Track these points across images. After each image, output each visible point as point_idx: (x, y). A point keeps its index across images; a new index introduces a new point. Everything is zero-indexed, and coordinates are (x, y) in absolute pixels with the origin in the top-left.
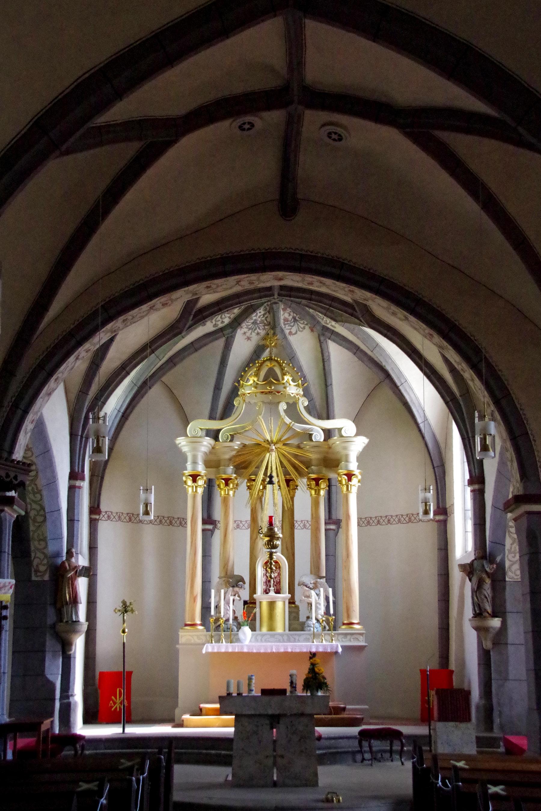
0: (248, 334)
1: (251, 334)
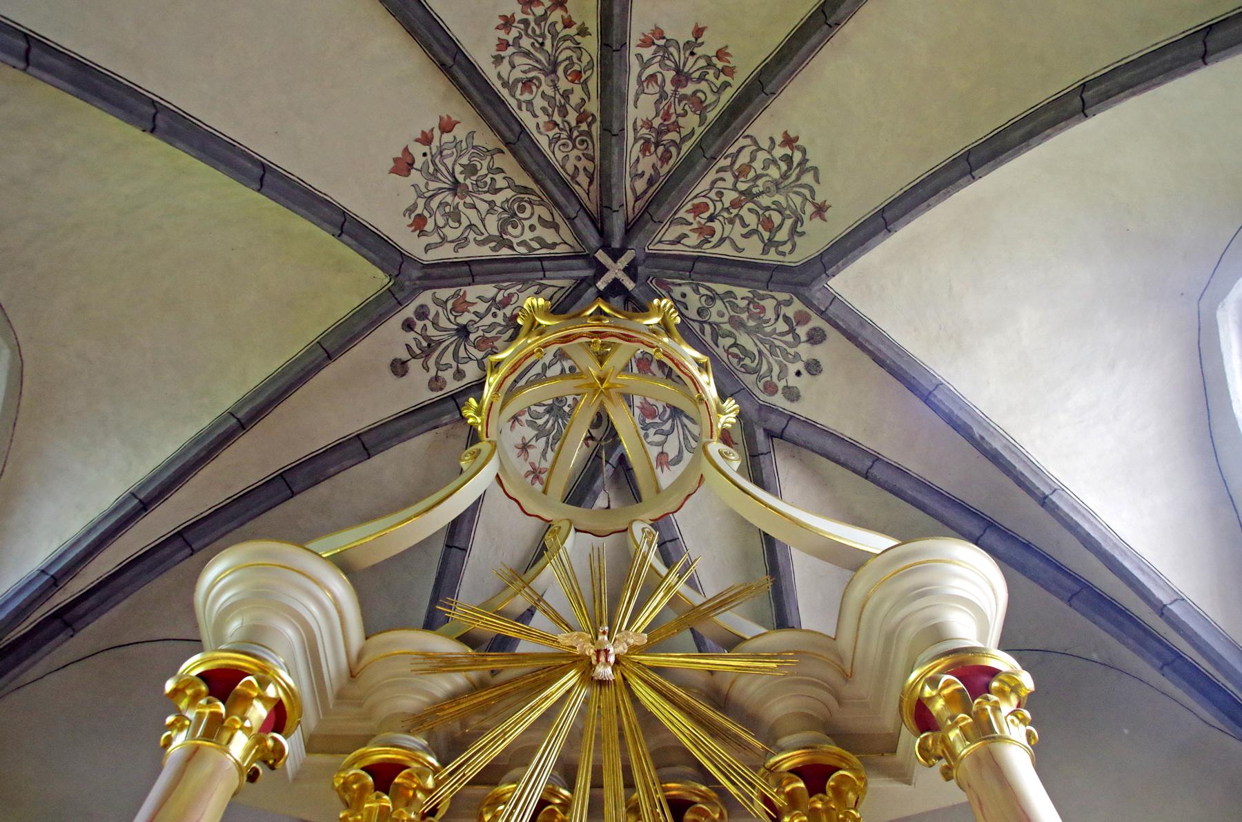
0: (534, 454)
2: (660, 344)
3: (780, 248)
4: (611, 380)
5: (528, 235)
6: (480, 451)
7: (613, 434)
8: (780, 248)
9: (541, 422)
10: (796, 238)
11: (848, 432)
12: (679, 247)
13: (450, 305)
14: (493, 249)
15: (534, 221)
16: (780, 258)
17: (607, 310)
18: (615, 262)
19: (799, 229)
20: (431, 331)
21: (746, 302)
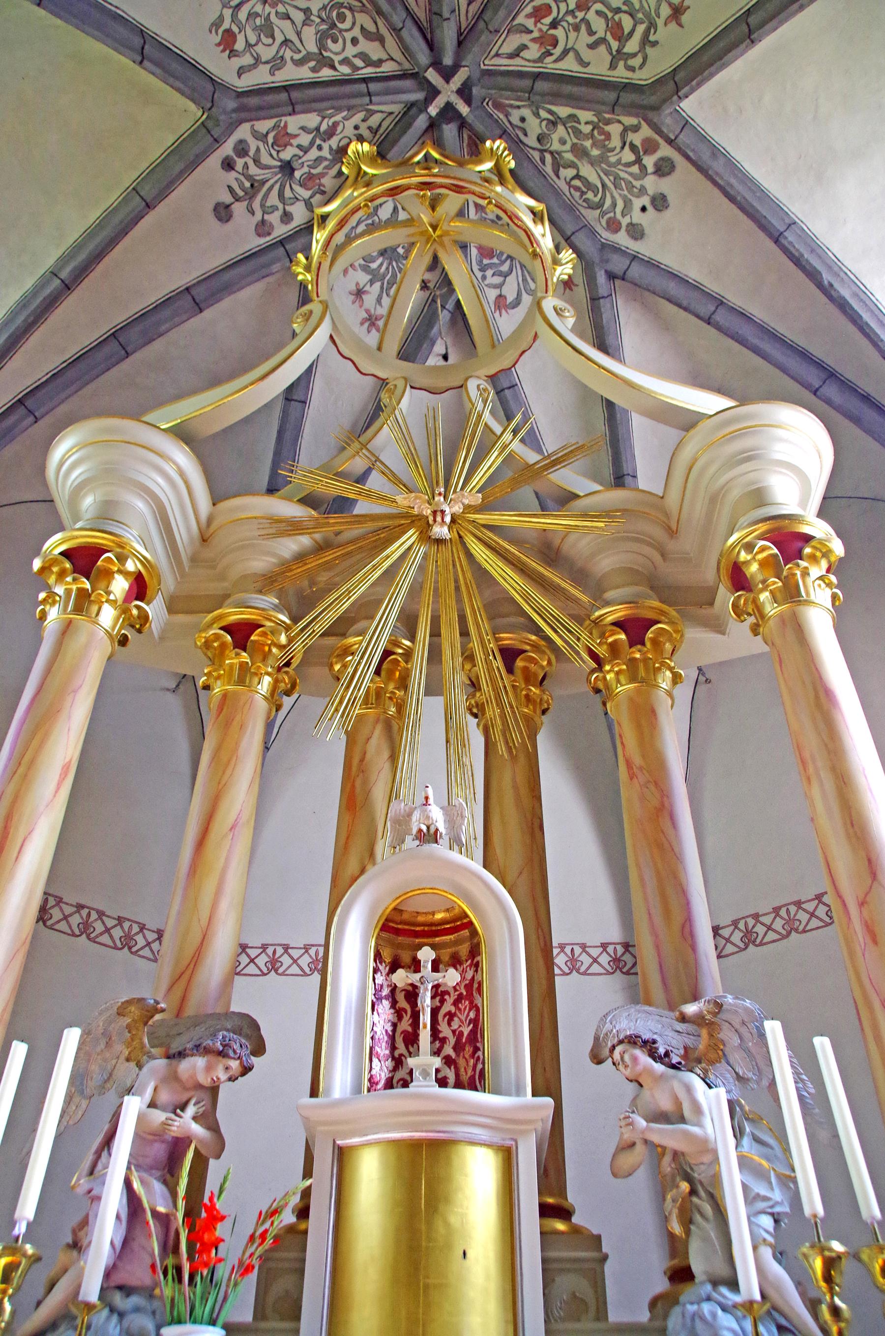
0: (369, 300)
1: (379, 300)
2: (492, 195)
3: (631, 62)
4: (443, 226)
5: (351, 51)
6: (311, 312)
7: (446, 282)
8: (631, 62)
9: (374, 266)
10: (649, 50)
11: (693, 273)
12: (517, 61)
13: (270, 139)
14: (314, 70)
15: (356, 32)
16: (629, 74)
17: (436, 155)
18: (448, 82)
19: (652, 38)
20: (253, 170)
21: (590, 127)
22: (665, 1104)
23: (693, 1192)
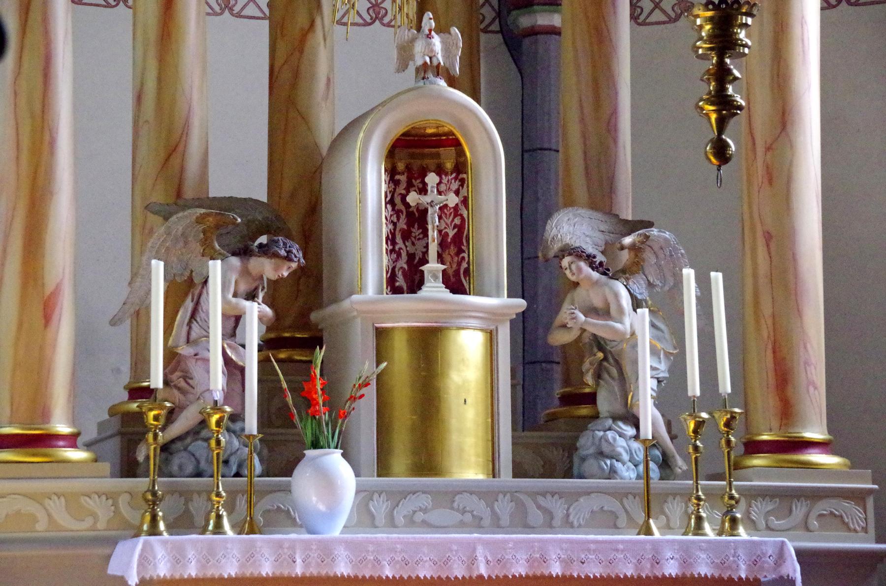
22: (598, 302)
23: (605, 359)
